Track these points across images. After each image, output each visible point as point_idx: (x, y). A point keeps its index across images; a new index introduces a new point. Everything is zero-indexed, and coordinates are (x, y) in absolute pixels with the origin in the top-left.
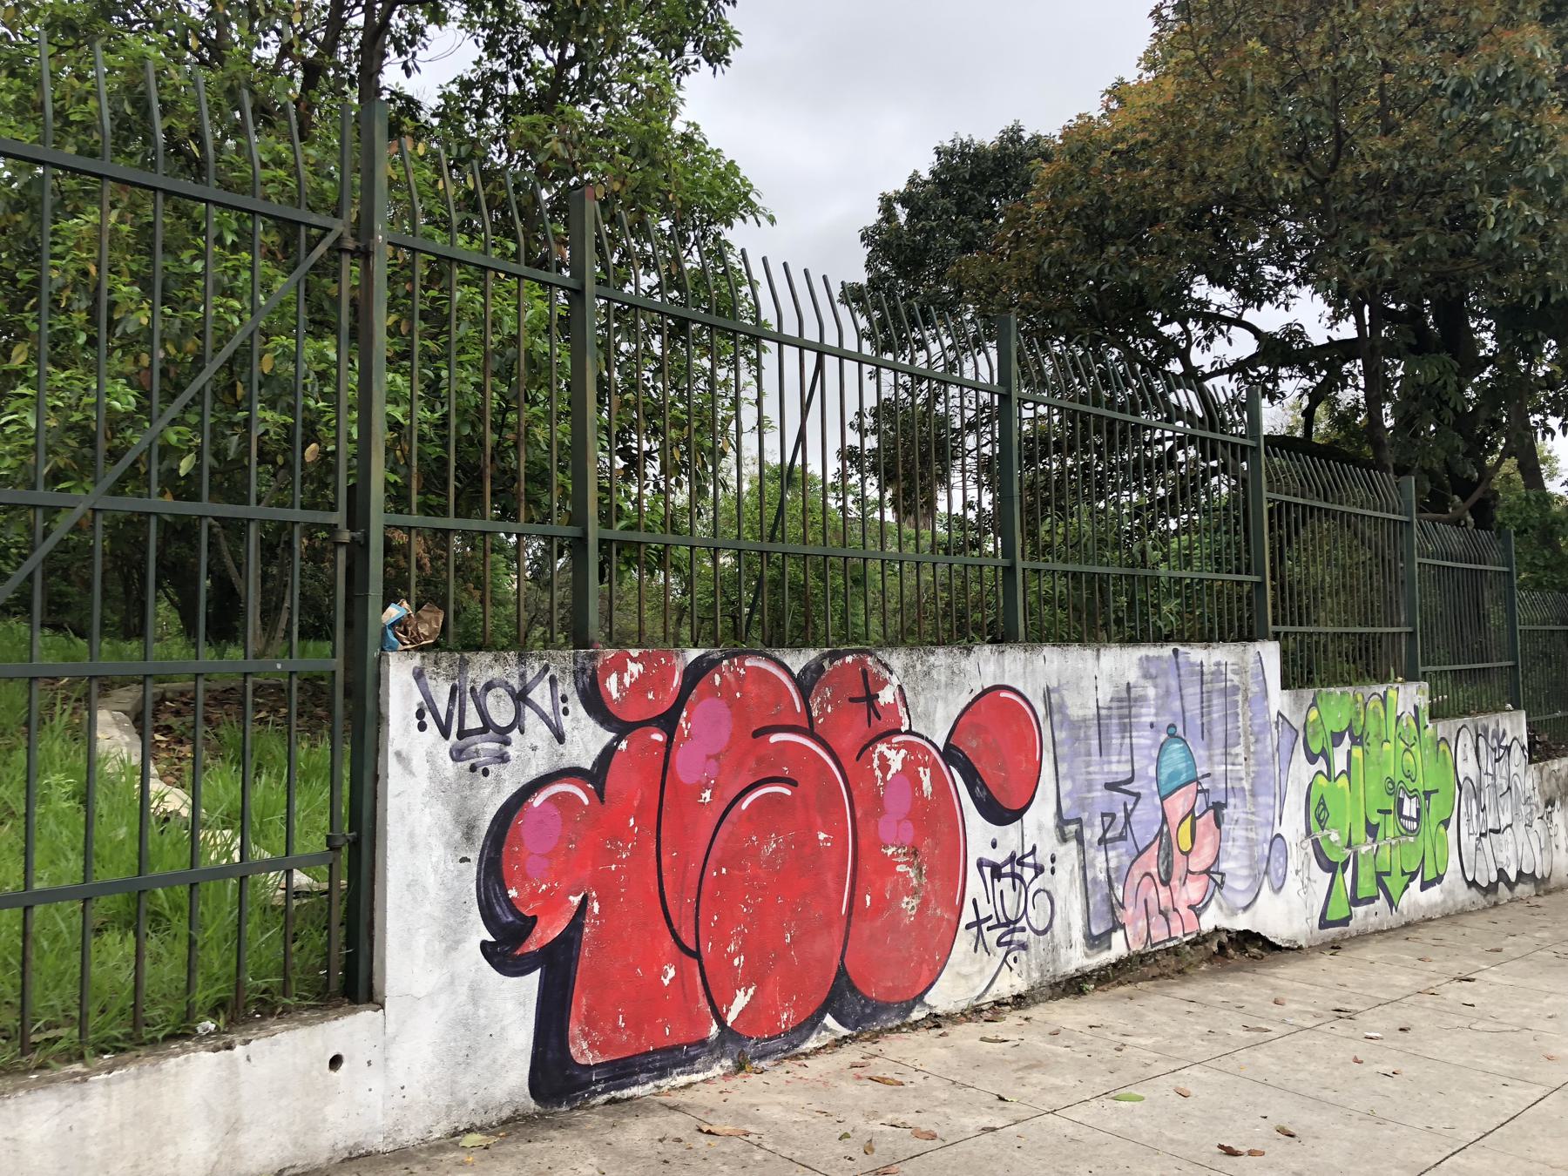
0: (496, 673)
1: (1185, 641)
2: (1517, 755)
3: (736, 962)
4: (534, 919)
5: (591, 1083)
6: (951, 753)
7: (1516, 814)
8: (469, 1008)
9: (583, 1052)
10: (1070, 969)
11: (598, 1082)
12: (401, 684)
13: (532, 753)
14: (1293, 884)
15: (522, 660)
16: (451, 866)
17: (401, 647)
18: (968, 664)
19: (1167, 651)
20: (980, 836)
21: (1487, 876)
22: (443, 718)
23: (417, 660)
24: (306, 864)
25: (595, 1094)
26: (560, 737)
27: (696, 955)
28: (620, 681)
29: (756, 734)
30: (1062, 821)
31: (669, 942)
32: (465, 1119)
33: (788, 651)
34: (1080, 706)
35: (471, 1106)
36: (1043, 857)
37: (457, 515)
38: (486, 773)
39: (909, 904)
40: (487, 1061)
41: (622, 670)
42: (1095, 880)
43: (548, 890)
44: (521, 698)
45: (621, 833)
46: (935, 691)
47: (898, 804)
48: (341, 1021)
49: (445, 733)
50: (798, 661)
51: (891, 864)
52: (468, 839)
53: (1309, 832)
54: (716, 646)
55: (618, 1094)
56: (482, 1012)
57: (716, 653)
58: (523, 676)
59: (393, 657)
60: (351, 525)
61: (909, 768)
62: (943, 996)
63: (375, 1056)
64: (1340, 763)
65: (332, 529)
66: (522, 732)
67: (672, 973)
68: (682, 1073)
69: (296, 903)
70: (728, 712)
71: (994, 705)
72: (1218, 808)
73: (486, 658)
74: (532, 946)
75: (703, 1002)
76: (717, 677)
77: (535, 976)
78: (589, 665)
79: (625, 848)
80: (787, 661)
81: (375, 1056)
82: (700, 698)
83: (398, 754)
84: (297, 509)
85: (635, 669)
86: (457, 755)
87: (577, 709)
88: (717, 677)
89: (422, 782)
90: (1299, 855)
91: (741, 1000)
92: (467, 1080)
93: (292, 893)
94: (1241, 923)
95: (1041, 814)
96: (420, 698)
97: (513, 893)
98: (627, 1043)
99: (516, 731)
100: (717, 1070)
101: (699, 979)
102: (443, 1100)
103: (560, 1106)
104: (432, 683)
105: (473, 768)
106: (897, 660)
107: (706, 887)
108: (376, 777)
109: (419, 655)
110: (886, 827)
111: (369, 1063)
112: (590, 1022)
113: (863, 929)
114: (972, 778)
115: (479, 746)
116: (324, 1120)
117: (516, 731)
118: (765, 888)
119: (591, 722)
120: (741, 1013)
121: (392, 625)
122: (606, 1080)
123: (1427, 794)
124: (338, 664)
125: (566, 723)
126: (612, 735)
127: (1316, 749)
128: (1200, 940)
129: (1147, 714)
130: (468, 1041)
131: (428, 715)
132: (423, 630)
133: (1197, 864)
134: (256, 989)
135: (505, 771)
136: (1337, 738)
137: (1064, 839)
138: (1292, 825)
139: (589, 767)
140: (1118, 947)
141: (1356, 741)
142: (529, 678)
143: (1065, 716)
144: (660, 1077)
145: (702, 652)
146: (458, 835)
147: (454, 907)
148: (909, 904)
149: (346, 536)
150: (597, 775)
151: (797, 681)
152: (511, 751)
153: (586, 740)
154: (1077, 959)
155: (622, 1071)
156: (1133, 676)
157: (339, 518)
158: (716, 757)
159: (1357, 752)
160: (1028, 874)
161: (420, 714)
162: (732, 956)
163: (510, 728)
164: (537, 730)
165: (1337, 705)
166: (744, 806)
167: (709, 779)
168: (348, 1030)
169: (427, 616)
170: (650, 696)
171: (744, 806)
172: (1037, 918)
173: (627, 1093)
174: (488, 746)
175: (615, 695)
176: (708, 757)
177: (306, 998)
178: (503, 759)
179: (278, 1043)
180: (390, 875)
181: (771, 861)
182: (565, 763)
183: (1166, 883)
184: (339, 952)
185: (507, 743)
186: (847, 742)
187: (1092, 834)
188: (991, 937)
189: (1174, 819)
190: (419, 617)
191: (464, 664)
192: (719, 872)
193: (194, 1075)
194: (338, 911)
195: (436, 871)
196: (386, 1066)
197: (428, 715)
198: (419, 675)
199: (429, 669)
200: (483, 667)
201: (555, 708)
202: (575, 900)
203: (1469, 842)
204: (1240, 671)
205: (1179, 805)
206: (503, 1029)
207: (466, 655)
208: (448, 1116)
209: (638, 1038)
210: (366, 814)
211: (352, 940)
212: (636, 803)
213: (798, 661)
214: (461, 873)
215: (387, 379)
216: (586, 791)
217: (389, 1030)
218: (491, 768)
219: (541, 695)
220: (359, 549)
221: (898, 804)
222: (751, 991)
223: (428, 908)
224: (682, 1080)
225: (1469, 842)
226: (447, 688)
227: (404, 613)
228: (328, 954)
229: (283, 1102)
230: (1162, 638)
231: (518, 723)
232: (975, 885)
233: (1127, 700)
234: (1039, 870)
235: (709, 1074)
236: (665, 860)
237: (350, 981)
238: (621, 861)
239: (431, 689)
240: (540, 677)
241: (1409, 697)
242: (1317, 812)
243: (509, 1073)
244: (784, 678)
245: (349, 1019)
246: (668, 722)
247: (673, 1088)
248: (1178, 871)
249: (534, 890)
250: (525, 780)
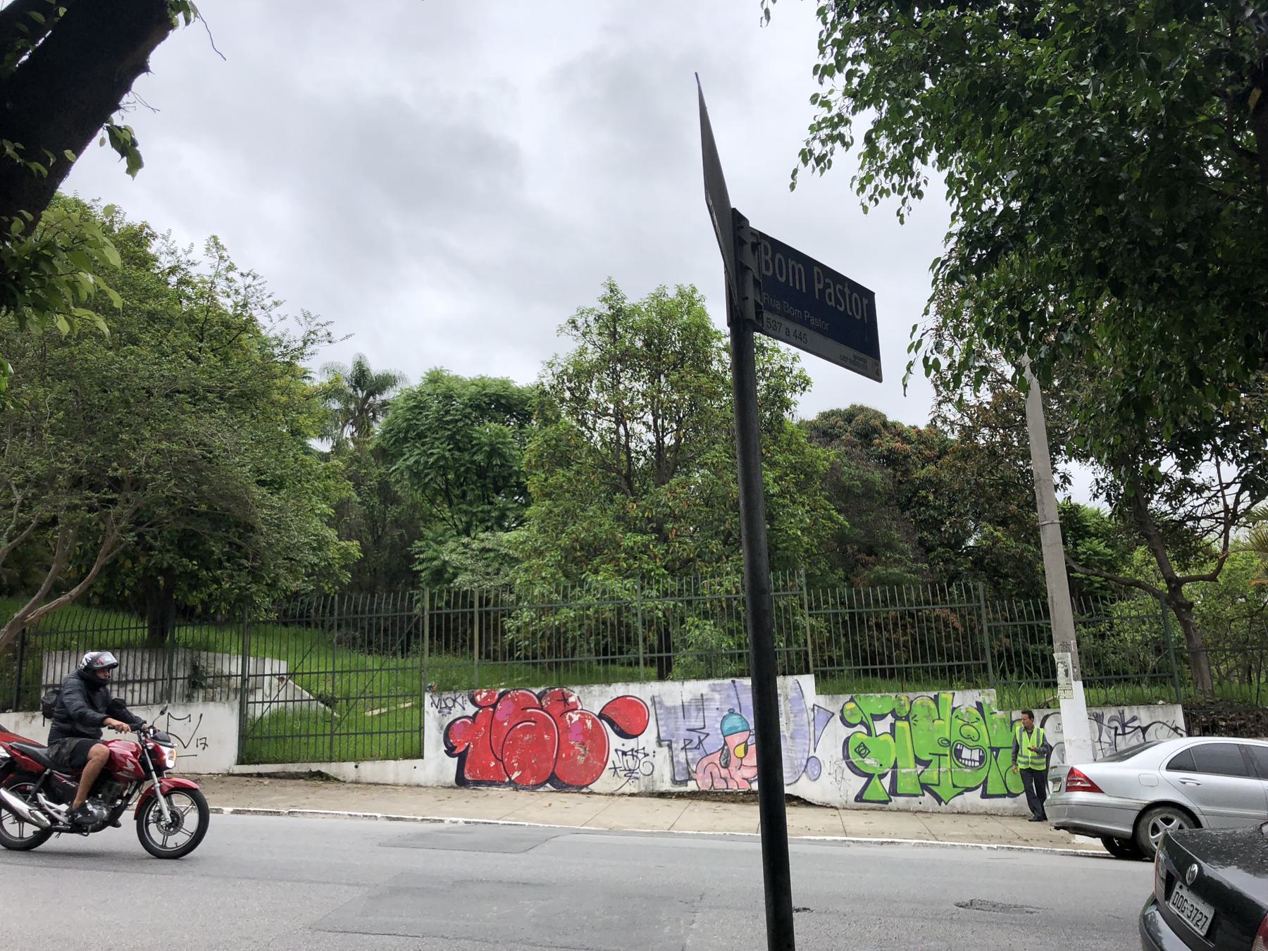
1: (736, 676)
6: (601, 716)
9: (468, 777)
13: (457, 712)
14: (825, 778)
19: (728, 681)
20: (615, 741)
30: (660, 741)
36: (649, 750)
39: (581, 759)
44: (454, 701)
46: (592, 699)
50: (537, 691)
51: (573, 747)
53: (846, 757)
61: (582, 721)
85: (484, 694)
91: (516, 774)
98: (479, 777)
106: (577, 689)
112: (470, 771)
114: (612, 724)
123: (997, 750)
136: (876, 717)
137: (660, 746)
140: (692, 786)
141: (897, 718)
147: (438, 742)
148: (581, 759)
153: (471, 710)
154: (667, 786)
155: (478, 783)
160: (641, 756)
164: (458, 707)
183: (726, 766)
186: (556, 712)
193: (391, 764)
213: (537, 691)
219: (460, 700)
232: (613, 756)
234: (646, 755)
237: (420, 756)
243: (451, 776)
246: (494, 706)
248: (734, 762)
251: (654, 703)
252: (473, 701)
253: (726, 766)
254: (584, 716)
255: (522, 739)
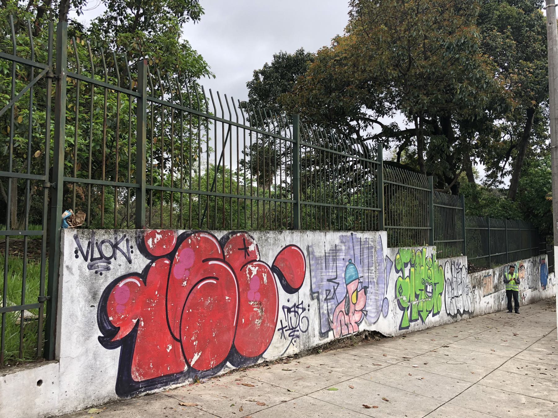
0: (106, 237)
1: (355, 231)
2: (464, 271)
3: (195, 343)
4: (119, 328)
5: (139, 388)
6: (274, 268)
7: (463, 291)
8: (93, 361)
9: (136, 377)
10: (314, 345)
11: (142, 388)
12: (69, 241)
13: (119, 267)
14: (390, 315)
15: (116, 233)
16: (87, 309)
17: (69, 227)
18: (281, 237)
19: (349, 233)
21: (453, 312)
22: (85, 254)
23: (75, 232)
24: (30, 308)
25: (141, 392)
26: (130, 262)
27: (180, 341)
28: (153, 241)
29: (204, 261)
30: (312, 293)
31: (170, 336)
32: (90, 403)
33: (216, 231)
34: (319, 252)
35: (93, 398)
36: (305, 305)
37: (92, 178)
38: (101, 274)
39: (258, 322)
40: (99, 381)
41: (154, 237)
42: (323, 313)
43: (124, 318)
44: (115, 247)
45: (153, 297)
46: (269, 247)
47: (255, 286)
48: (42, 368)
49: (86, 259)
50: (220, 235)
51: (252, 307)
52: (94, 299)
53: (396, 297)
54: (190, 229)
55: (150, 392)
56: (98, 363)
57: (189, 232)
58: (116, 238)
59: (66, 231)
60: (51, 180)
62: (269, 355)
63: (55, 380)
64: (407, 273)
65: (43, 182)
66: (115, 259)
67: (170, 347)
68: (174, 384)
69: (25, 323)
70: (193, 253)
71: (290, 251)
72: (365, 288)
73: (103, 231)
74: (118, 338)
75: (182, 358)
76: (190, 241)
77: (119, 349)
78: (141, 235)
79: (154, 302)
80: (216, 235)
81: (55, 380)
82: (183, 248)
83: (67, 267)
84: (29, 174)
85: (159, 237)
86: (90, 267)
87: (137, 251)
88: (190, 240)
89: (76, 277)
90: (393, 305)
91: (196, 357)
92: (91, 388)
93: (23, 319)
94: (373, 328)
95: (305, 290)
96: (76, 246)
97: (111, 319)
98: (153, 373)
99: (113, 259)
100: (187, 382)
101: (181, 350)
102: (81, 396)
103: (127, 396)
104: (81, 240)
105: (96, 272)
106: (256, 235)
107: (184, 316)
108: (59, 275)
109: (76, 230)
110: (250, 295)
111: (53, 383)
112: (139, 365)
113: (241, 331)
115: (99, 264)
116: (35, 404)
117: (113, 259)
118: (204, 316)
119: (142, 256)
120: (196, 362)
121: (66, 219)
122: (145, 387)
123: (435, 284)
124: (44, 233)
125: (132, 256)
126: (149, 261)
127: (399, 268)
128: (359, 334)
129: (342, 255)
130: (92, 372)
131: (79, 252)
132: (78, 221)
133: (359, 307)
134: (8, 356)
135: (109, 274)
136: (406, 265)
137: (313, 299)
138: (391, 294)
139: (141, 272)
140: (331, 337)
141: (412, 266)
142: (118, 239)
143: (314, 255)
144: (166, 385)
145: (184, 231)
146: (90, 297)
147: (88, 324)
148: (258, 322)
149: (48, 185)
150: (144, 276)
151: (219, 242)
152: (111, 266)
153: (140, 263)
154: (316, 341)
155: (151, 384)
156: (337, 242)
157: (46, 178)
158: (189, 269)
159: (412, 269)
160: (300, 311)
161: (76, 252)
162: (193, 341)
163: (111, 258)
165: (406, 254)
166: (199, 287)
167: (186, 277)
168: (45, 371)
169: (79, 215)
170: (164, 247)
171: (199, 287)
172: (303, 327)
173: (153, 391)
174: (102, 264)
175: (151, 246)
176: (186, 269)
177: (28, 359)
178: (108, 269)
179: (17, 375)
180: (63, 312)
181: (208, 307)
182: (131, 271)
183: (347, 314)
184: (42, 341)
185: (110, 263)
186: (237, 264)
187: (323, 297)
188: (287, 333)
189: (351, 292)
190: (76, 216)
191: (94, 234)
192: (189, 311)
194: (42, 326)
195: (81, 310)
196: (60, 384)
197: (79, 252)
198: (76, 237)
199: (80, 235)
200: (101, 235)
201: (128, 250)
202: (135, 321)
203: (448, 300)
204: (374, 241)
205: (352, 287)
206: (106, 369)
207: (94, 230)
208: (84, 402)
209: (157, 372)
210: (54, 289)
211: (47, 336)
212: (158, 286)
213: (220, 235)
214: (91, 311)
215: (65, 128)
216: (139, 281)
217: (61, 370)
218: (103, 272)
219: (123, 245)
220: (53, 190)
221: (255, 286)
222: (200, 354)
223: (78, 324)
224: (174, 386)
225: (448, 300)
226: (87, 242)
227: (71, 214)
228: (37, 342)
229: (19, 398)
230: (347, 229)
231: (114, 256)
232: (281, 315)
233: (335, 250)
234: (304, 310)
235: (184, 384)
236: (169, 306)
238: (152, 307)
239: (81, 243)
240: (122, 239)
241: (430, 251)
242: (399, 290)
244: (215, 241)
245: (45, 366)
246: (171, 256)
247: (170, 389)
248: (352, 310)
249: (119, 318)
250: (116, 277)
251: (309, 254)
252: (143, 249)
253: (347, 314)
254: (262, 268)
255: (202, 304)
